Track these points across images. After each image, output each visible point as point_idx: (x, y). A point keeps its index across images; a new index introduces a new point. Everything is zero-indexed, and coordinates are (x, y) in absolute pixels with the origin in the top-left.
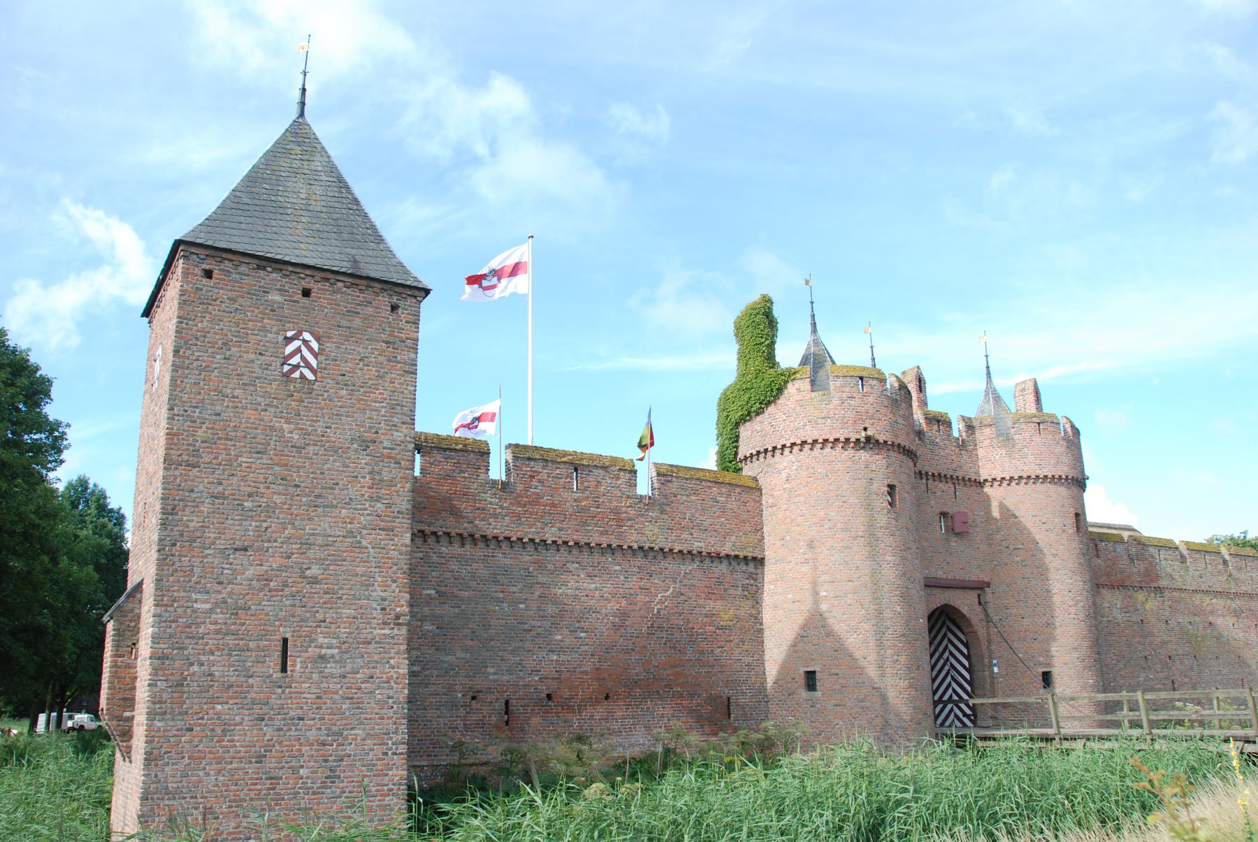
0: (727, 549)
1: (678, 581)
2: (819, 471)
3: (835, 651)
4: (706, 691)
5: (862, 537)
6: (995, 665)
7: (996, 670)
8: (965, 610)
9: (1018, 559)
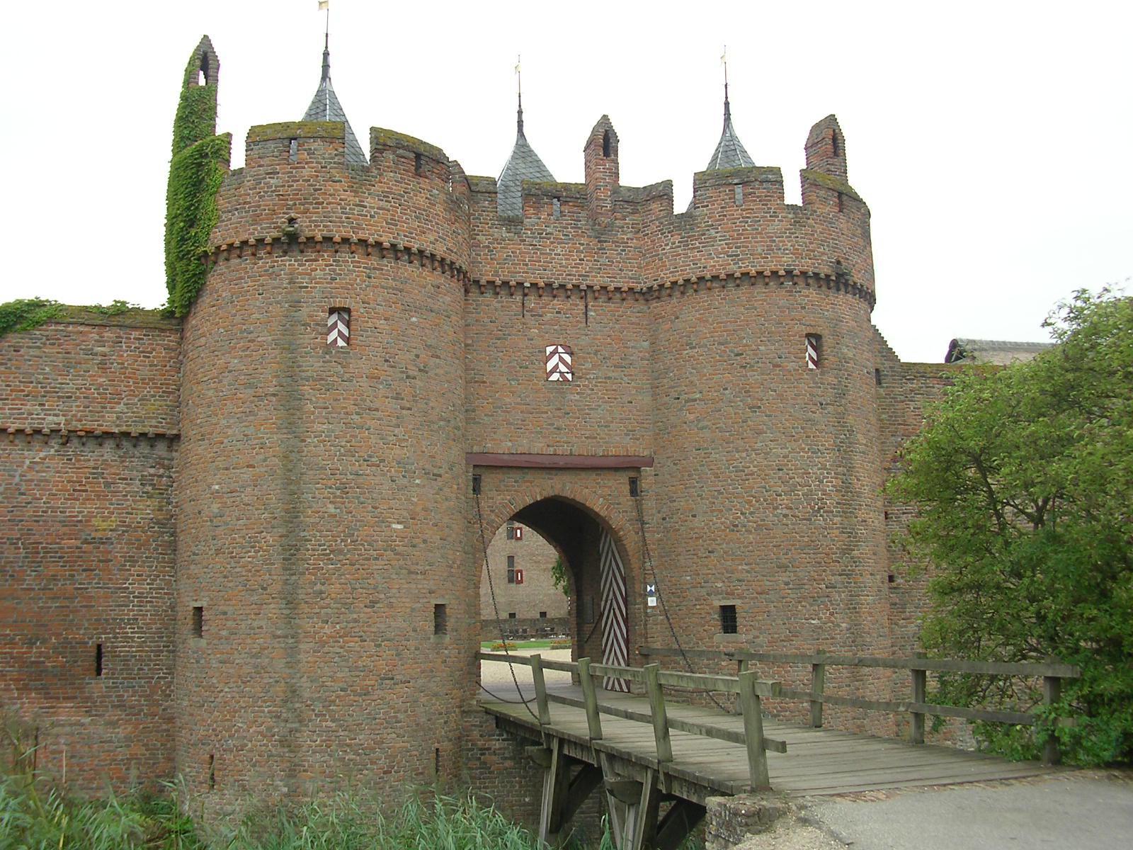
0: (109, 422)
1: (17, 474)
2: (224, 295)
3: (225, 577)
4: (58, 635)
5: (274, 395)
6: (651, 593)
7: (652, 601)
8: (597, 504)
9: (692, 417)
